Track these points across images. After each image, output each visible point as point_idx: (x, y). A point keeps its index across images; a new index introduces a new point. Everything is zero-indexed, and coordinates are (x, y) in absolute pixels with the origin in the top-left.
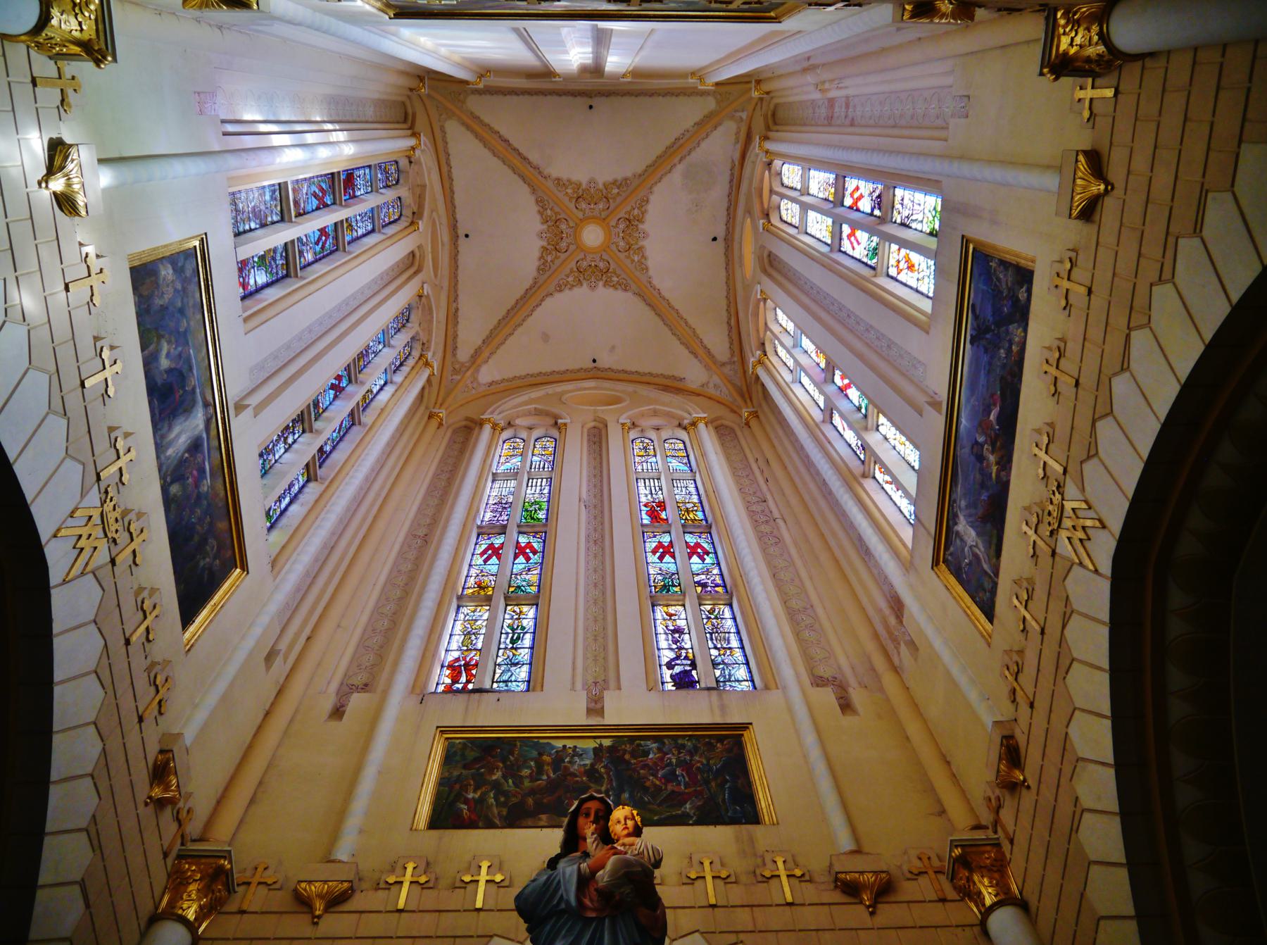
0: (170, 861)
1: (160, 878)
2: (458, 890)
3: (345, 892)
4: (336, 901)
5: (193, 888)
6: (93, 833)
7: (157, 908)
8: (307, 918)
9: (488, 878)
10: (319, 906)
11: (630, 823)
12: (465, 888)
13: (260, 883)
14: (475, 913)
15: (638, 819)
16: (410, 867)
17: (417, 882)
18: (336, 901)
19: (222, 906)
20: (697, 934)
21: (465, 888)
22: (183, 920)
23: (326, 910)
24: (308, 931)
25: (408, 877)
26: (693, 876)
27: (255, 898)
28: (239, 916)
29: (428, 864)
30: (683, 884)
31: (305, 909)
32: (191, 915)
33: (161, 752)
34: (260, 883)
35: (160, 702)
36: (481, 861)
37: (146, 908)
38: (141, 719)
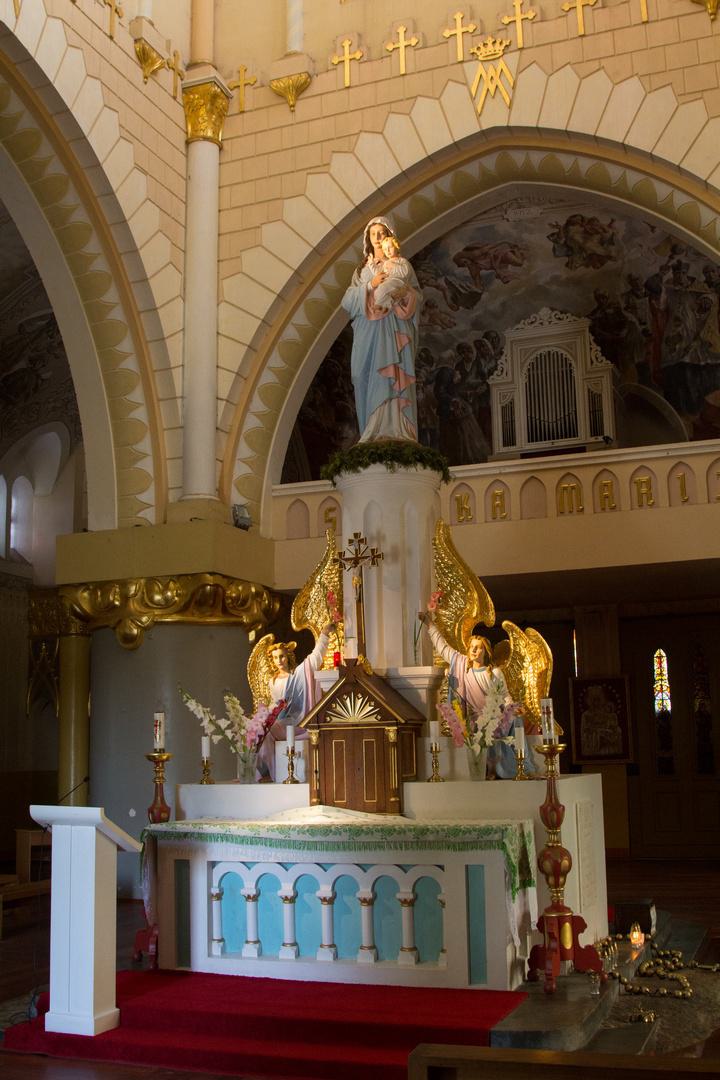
0: (179, 99)
1: (178, 113)
2: (385, 59)
3: (305, 82)
4: (301, 89)
5: (202, 112)
6: (127, 135)
7: (187, 133)
8: (285, 108)
9: (406, 43)
10: (291, 98)
11: (392, 250)
12: (390, 56)
13: (245, 85)
14: (401, 78)
15: (396, 245)
16: (347, 44)
17: (354, 59)
18: (301, 89)
19: (226, 111)
20: (568, 66)
21: (390, 56)
22: (206, 139)
23: (297, 99)
24: (289, 118)
25: (347, 57)
26: (567, 9)
27: (247, 98)
28: (241, 116)
29: (360, 35)
30: (560, 17)
31: (283, 101)
32: (210, 134)
33: (136, 41)
34: (245, 85)
35: (116, 11)
36: (398, 28)
37: (182, 138)
38: (111, 38)
